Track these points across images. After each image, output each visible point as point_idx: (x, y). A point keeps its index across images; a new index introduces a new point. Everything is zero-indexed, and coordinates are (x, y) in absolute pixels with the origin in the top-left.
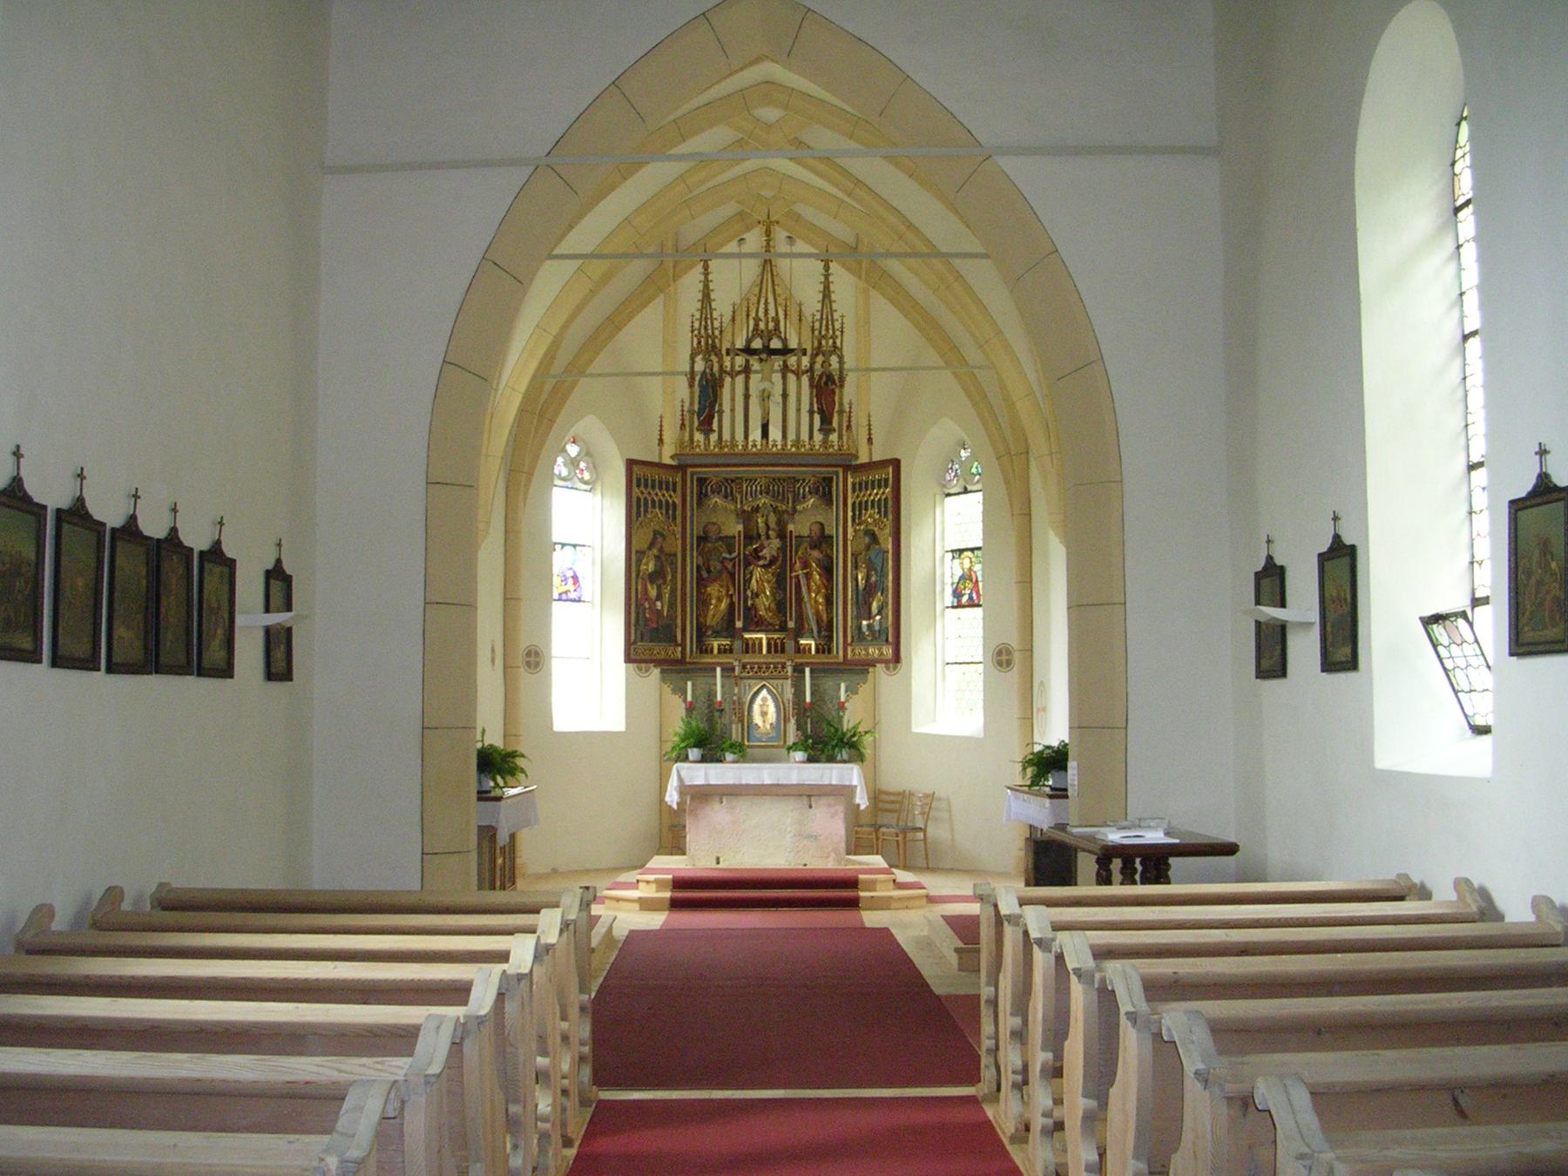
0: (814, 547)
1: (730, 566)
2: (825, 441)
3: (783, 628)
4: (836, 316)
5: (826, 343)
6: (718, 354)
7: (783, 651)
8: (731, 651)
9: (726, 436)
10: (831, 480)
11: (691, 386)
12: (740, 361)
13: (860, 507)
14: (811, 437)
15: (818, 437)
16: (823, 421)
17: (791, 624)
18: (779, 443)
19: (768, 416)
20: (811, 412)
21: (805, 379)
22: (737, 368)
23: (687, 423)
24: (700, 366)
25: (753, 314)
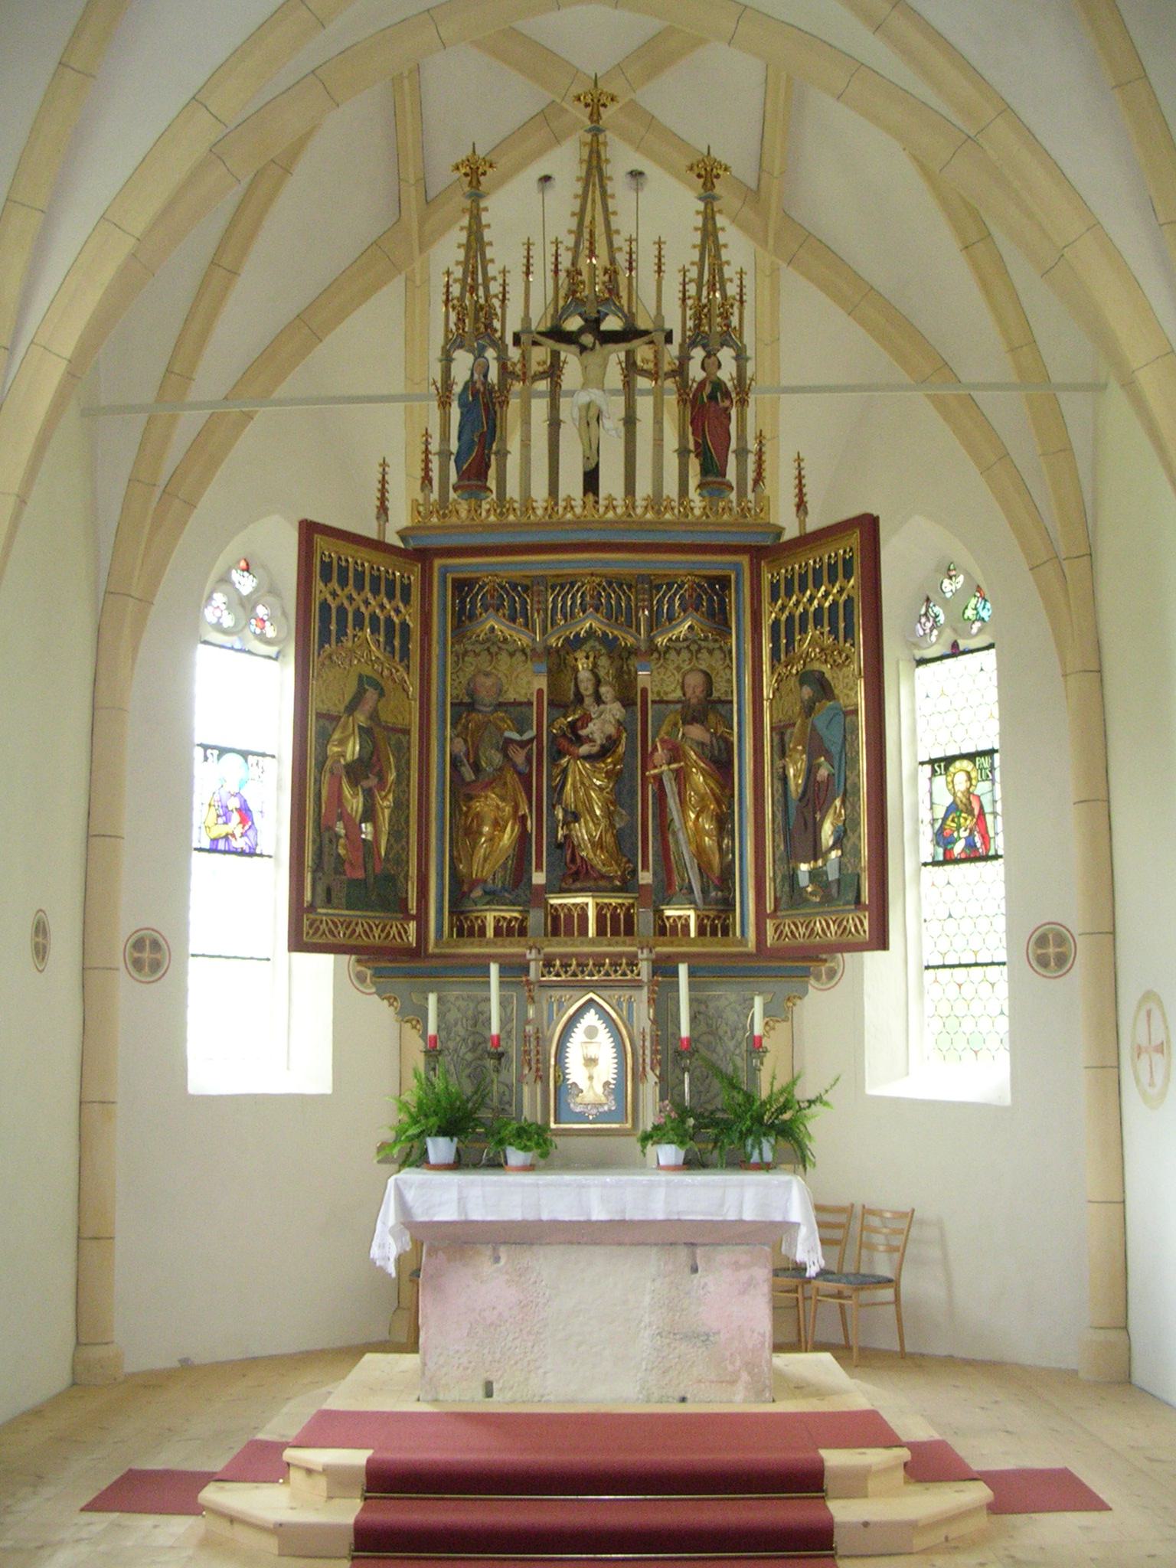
1: (519, 757)
4: (728, 272)
6: (500, 346)
7: (629, 931)
8: (523, 932)
9: (513, 490)
10: (724, 582)
11: (444, 404)
12: (540, 355)
13: (787, 631)
16: (705, 471)
17: (645, 878)
18: (619, 502)
20: (683, 453)
22: (535, 368)
23: (435, 475)
24: (463, 364)
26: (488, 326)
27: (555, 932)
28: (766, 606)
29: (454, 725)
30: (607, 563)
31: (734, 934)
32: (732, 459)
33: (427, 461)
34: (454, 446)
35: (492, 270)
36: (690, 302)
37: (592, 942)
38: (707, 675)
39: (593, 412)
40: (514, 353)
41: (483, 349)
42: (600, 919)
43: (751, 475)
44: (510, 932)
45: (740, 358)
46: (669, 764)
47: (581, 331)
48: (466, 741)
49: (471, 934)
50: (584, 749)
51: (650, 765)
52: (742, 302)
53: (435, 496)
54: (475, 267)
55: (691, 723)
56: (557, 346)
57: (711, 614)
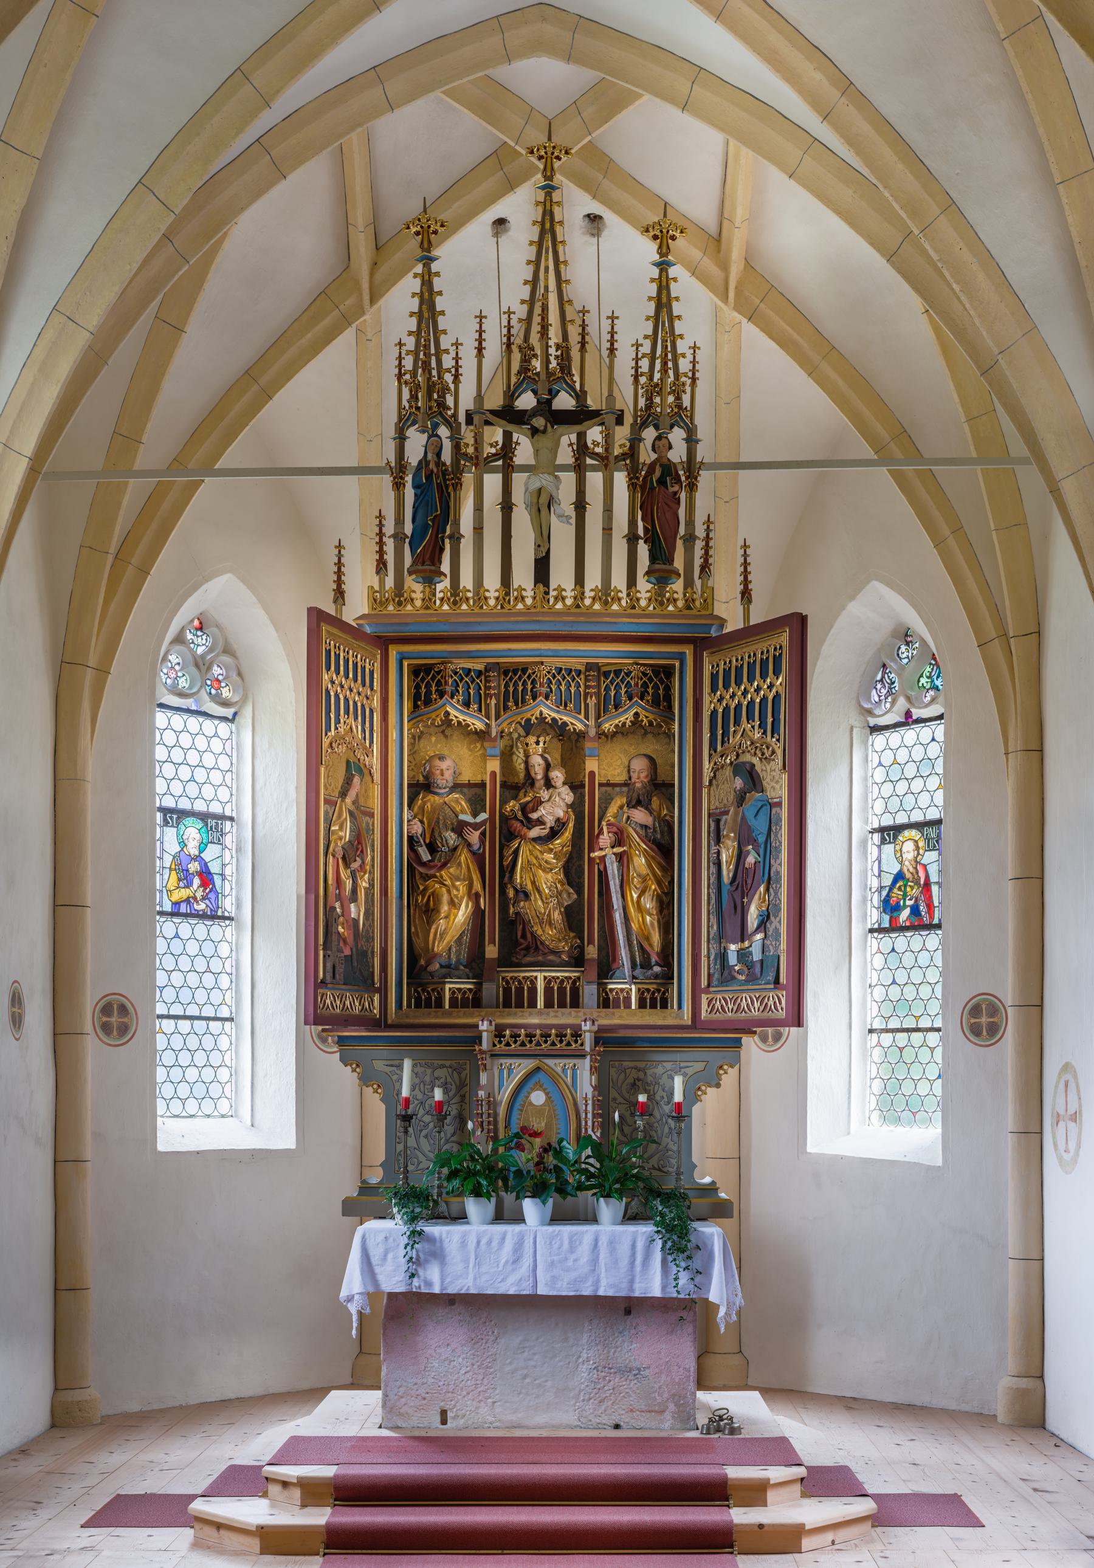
0: (636, 803)
1: (474, 837)
2: (659, 598)
3: (578, 960)
4: (682, 346)
5: (666, 400)
7: (576, 1003)
9: (467, 581)
10: (668, 671)
11: (398, 485)
12: (495, 435)
14: (632, 582)
15: (644, 586)
16: (653, 559)
18: (569, 594)
19: (550, 550)
20: (632, 539)
21: (620, 479)
23: (390, 557)
24: (416, 444)
25: (518, 340)
26: (442, 405)
27: (507, 1004)
28: (706, 698)
29: (409, 806)
30: (556, 654)
31: (672, 1007)
32: (679, 544)
33: (381, 543)
34: (408, 529)
35: (445, 342)
36: (643, 380)
37: (540, 1013)
38: (651, 759)
39: (544, 500)
40: (467, 435)
41: (436, 426)
42: (548, 990)
43: (698, 562)
44: (465, 1004)
45: (691, 440)
46: (613, 847)
47: (534, 413)
48: (422, 822)
49: (428, 1005)
50: (535, 832)
51: (596, 848)
52: (694, 379)
53: (390, 582)
54: (428, 340)
55: (634, 807)
56: (510, 427)
57: (656, 703)
